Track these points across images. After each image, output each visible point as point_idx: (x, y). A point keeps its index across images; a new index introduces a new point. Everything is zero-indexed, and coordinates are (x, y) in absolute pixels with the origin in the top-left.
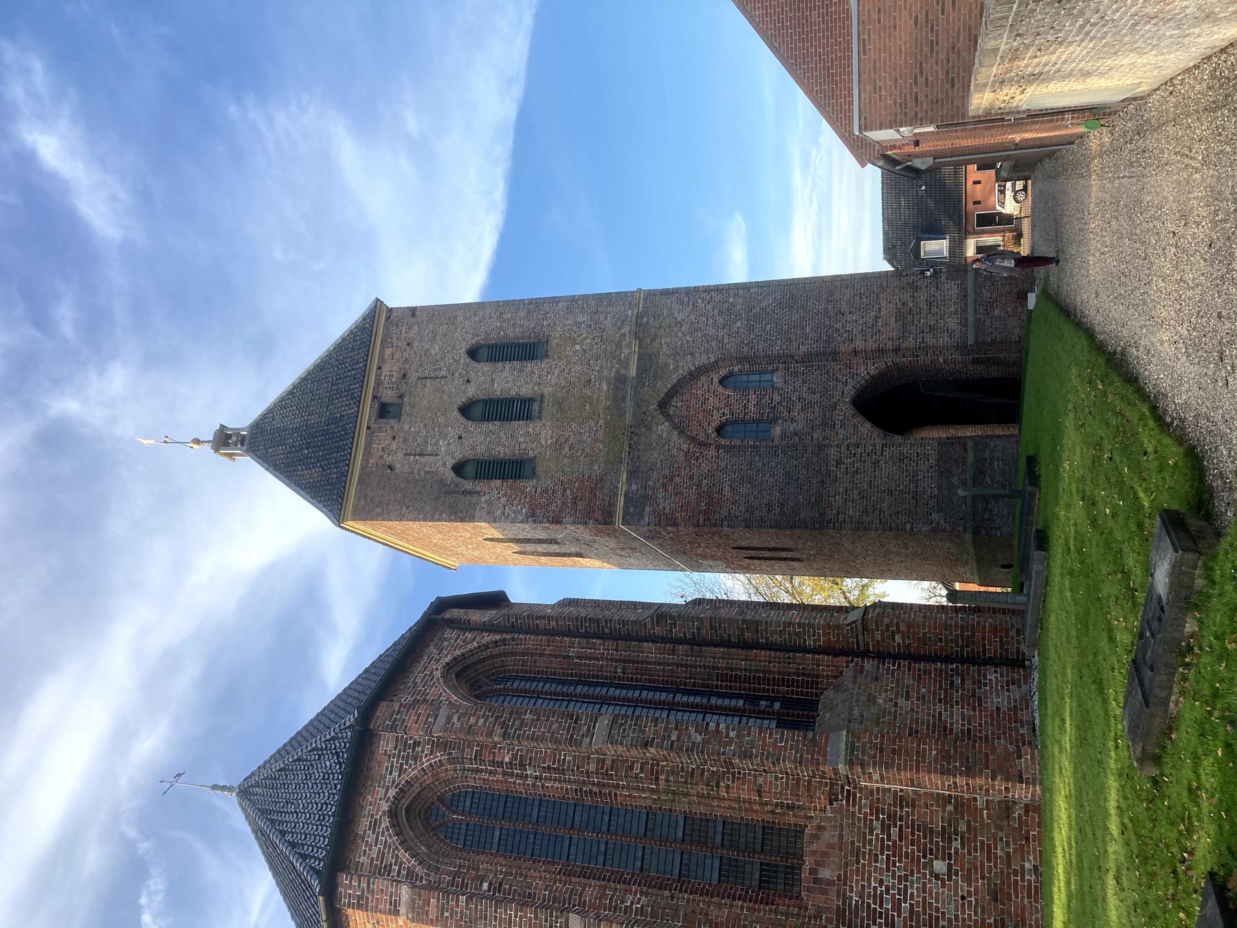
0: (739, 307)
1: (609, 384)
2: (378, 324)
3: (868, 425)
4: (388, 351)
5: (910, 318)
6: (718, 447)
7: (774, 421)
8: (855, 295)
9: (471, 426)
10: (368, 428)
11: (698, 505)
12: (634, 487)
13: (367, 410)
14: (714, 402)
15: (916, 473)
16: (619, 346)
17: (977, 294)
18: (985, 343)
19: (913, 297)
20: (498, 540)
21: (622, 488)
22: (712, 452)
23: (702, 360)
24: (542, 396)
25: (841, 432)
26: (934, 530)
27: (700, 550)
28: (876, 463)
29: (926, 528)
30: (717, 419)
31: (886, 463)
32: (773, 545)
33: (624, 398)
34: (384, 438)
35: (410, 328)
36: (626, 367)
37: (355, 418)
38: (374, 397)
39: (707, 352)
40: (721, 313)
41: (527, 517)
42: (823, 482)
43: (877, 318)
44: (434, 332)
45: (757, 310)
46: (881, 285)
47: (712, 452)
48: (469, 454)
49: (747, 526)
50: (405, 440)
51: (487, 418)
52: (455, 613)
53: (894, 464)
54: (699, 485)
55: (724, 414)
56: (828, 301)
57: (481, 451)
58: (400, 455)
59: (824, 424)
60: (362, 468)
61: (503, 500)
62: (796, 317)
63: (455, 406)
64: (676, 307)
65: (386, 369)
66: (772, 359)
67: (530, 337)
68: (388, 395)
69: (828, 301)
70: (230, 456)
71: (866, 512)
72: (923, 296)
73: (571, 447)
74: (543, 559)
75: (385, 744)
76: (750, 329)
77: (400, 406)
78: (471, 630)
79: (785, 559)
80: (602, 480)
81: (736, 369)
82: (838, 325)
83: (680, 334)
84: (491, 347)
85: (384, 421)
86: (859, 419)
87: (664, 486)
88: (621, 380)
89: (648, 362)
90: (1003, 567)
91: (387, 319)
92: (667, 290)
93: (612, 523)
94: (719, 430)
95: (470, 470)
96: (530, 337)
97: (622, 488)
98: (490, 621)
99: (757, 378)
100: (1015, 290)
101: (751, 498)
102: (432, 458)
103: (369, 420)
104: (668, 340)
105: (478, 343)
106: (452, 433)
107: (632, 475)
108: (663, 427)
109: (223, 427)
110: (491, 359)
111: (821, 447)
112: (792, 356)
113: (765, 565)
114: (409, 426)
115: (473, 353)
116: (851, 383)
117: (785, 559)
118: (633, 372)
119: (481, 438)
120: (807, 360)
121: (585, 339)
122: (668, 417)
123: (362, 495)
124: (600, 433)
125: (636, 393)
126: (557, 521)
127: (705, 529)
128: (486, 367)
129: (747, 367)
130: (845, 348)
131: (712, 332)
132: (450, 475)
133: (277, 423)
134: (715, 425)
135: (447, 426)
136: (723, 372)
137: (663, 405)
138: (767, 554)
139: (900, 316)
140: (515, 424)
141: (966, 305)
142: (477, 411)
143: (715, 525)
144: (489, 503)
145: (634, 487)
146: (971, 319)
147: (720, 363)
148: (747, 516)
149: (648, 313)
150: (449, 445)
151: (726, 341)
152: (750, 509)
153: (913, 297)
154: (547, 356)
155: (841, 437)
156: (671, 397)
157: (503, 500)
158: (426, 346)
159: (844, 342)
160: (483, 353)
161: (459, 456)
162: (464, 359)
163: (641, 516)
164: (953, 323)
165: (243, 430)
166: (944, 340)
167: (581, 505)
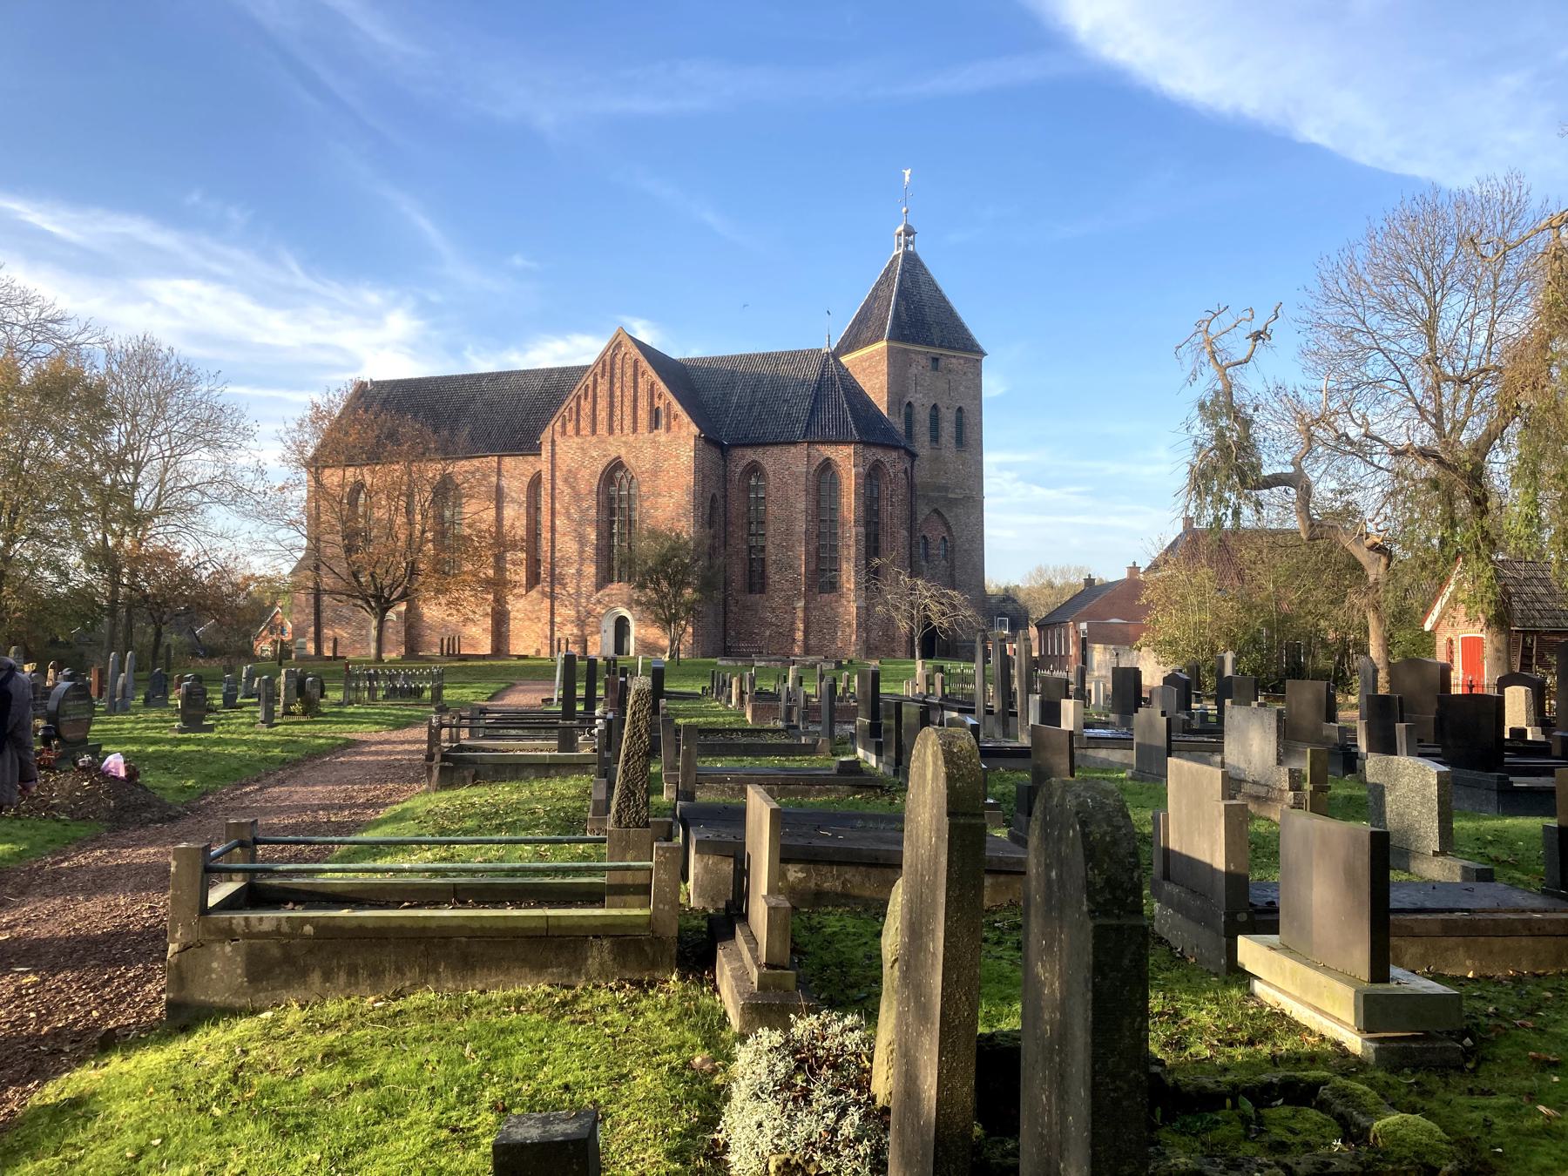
2: (970, 350)
30: (929, 535)
37: (931, 344)
66: (953, 561)
68: (942, 363)
75: (894, 454)
88: (945, 489)
89: (953, 503)
115: (960, 409)
132: (907, 400)
137: (936, 511)
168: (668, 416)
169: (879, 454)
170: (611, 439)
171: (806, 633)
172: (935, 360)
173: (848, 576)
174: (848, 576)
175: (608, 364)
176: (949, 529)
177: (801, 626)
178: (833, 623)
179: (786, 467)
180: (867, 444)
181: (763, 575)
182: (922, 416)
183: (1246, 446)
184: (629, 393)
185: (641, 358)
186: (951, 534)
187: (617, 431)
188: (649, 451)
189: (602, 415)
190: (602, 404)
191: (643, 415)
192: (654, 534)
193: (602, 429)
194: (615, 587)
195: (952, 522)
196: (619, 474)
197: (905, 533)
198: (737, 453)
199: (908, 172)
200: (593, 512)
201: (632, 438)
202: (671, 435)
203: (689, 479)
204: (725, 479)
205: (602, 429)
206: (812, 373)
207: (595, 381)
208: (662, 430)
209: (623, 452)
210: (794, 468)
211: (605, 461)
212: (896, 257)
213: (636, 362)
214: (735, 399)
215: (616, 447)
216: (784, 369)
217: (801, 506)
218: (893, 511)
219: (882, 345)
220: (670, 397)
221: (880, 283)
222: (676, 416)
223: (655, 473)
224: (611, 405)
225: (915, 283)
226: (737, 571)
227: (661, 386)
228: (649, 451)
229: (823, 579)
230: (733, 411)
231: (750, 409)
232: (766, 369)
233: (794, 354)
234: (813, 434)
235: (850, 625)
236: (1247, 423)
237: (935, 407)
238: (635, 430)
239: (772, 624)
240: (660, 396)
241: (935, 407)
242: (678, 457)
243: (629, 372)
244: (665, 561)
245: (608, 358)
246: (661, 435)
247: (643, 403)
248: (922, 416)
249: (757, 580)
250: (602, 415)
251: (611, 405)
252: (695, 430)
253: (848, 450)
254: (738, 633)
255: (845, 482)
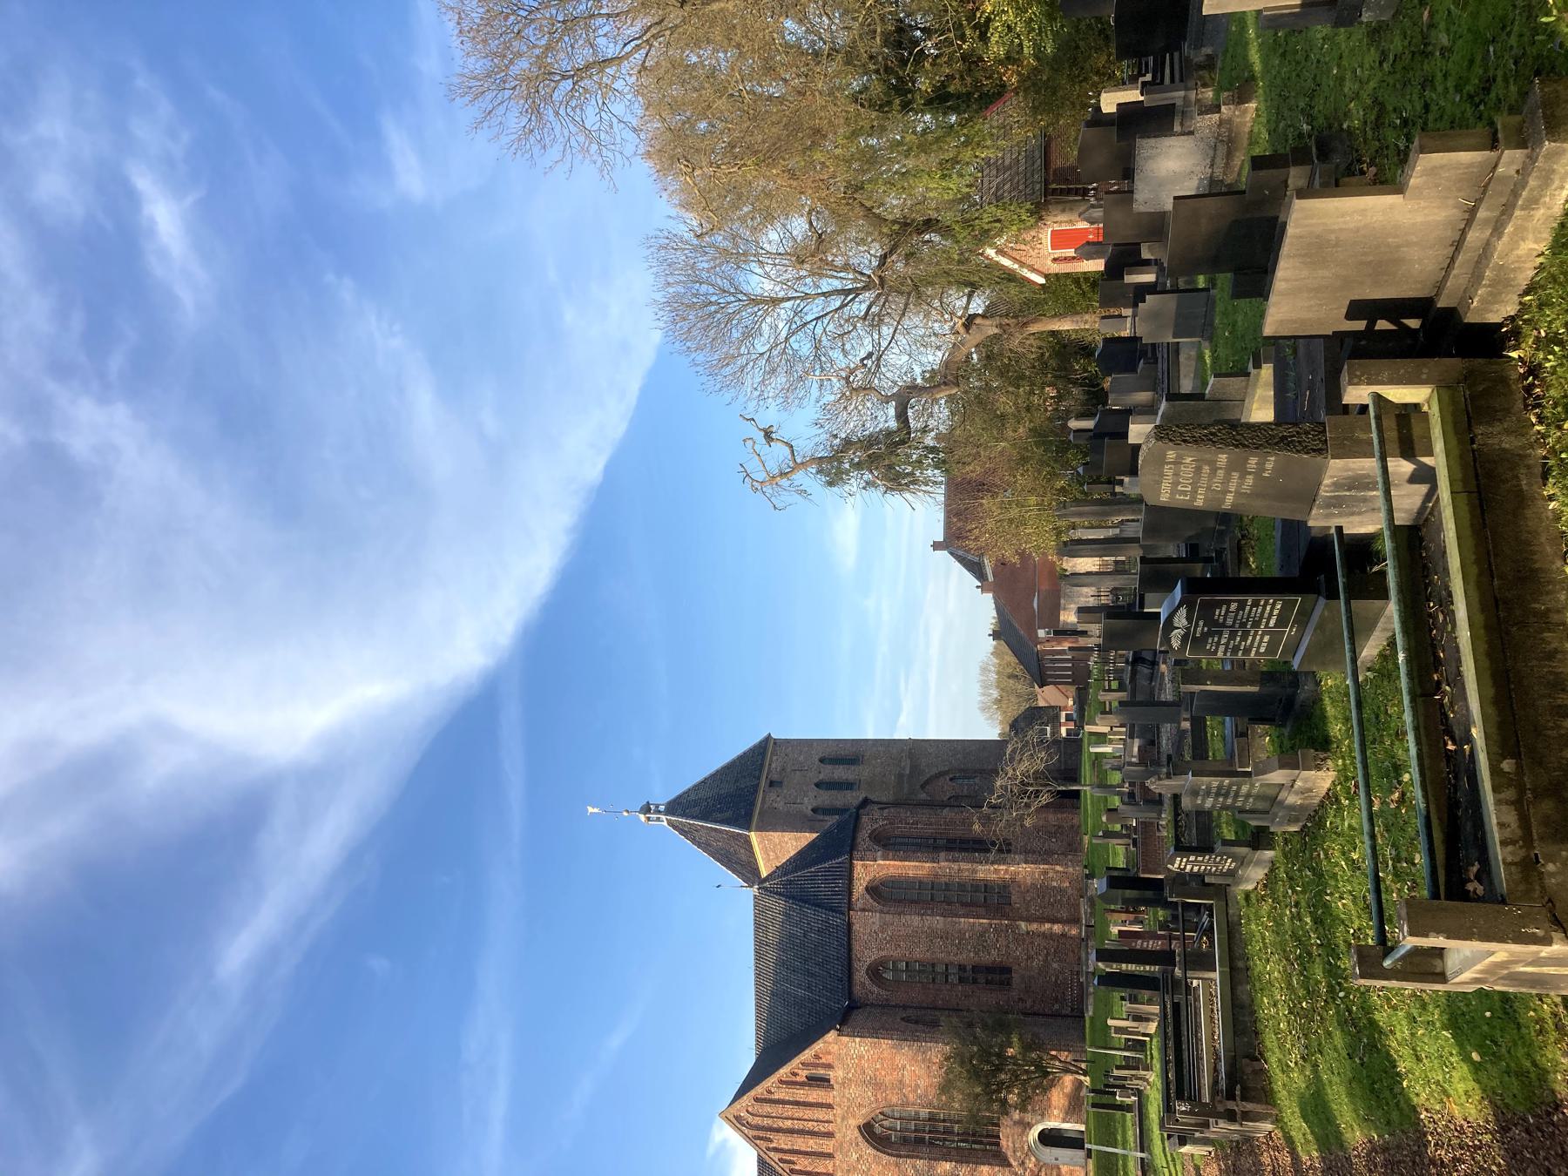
2: (766, 747)
37: (756, 788)
68: (775, 777)
75: (864, 819)
88: (900, 776)
89: (915, 768)
115: (822, 760)
132: (810, 813)
133: (693, 797)
137: (923, 787)
168: (816, 1066)
169: (864, 835)
170: (838, 1135)
171: (1054, 921)
173: (989, 871)
174: (989, 871)
175: (757, 1133)
176: (942, 774)
177: (1047, 926)
178: (1041, 890)
179: (874, 935)
180: (853, 847)
181: (990, 969)
182: (826, 798)
183: (870, 442)
184: (790, 1111)
185: (752, 1093)
187: (830, 1127)
188: (853, 1091)
189: (812, 1144)
190: (801, 1143)
191: (814, 1095)
192: (945, 1087)
193: (827, 1146)
194: (1006, 1143)
195: (934, 771)
196: (878, 1129)
197: (946, 811)
198: (857, 990)
199: (590, 810)
200: (919, 1163)
201: (838, 1111)
202: (836, 1063)
203: (885, 1044)
204: (885, 1006)
205: (827, 1146)
206: (777, 905)
207: (776, 1150)
208: (831, 1074)
209: (853, 1122)
210: (876, 927)
211: (863, 1145)
212: (669, 822)
213: (757, 1100)
214: (801, 992)
215: (848, 1130)
216: (773, 936)
217: (915, 920)
218: (923, 822)
219: (753, 836)
220: (796, 1062)
221: (694, 841)
222: (817, 1056)
223: (877, 1085)
224: (801, 1132)
225: (696, 803)
226: (991, 998)
227: (783, 1072)
228: (853, 1091)
229: (994, 900)
230: (813, 994)
231: (812, 975)
232: (772, 956)
233: (758, 925)
234: (841, 904)
235: (1045, 873)
236: (847, 443)
237: (817, 785)
238: (829, 1106)
239: (1045, 961)
240: (795, 1074)
241: (817, 785)
242: (861, 1057)
243: (768, 1108)
244: (975, 1074)
245: (751, 1133)
246: (836, 1075)
247: (801, 1094)
248: (826, 798)
249: (998, 975)
250: (812, 1144)
251: (801, 1132)
252: (831, 1036)
253: (858, 864)
254: (1056, 1000)
255: (892, 871)
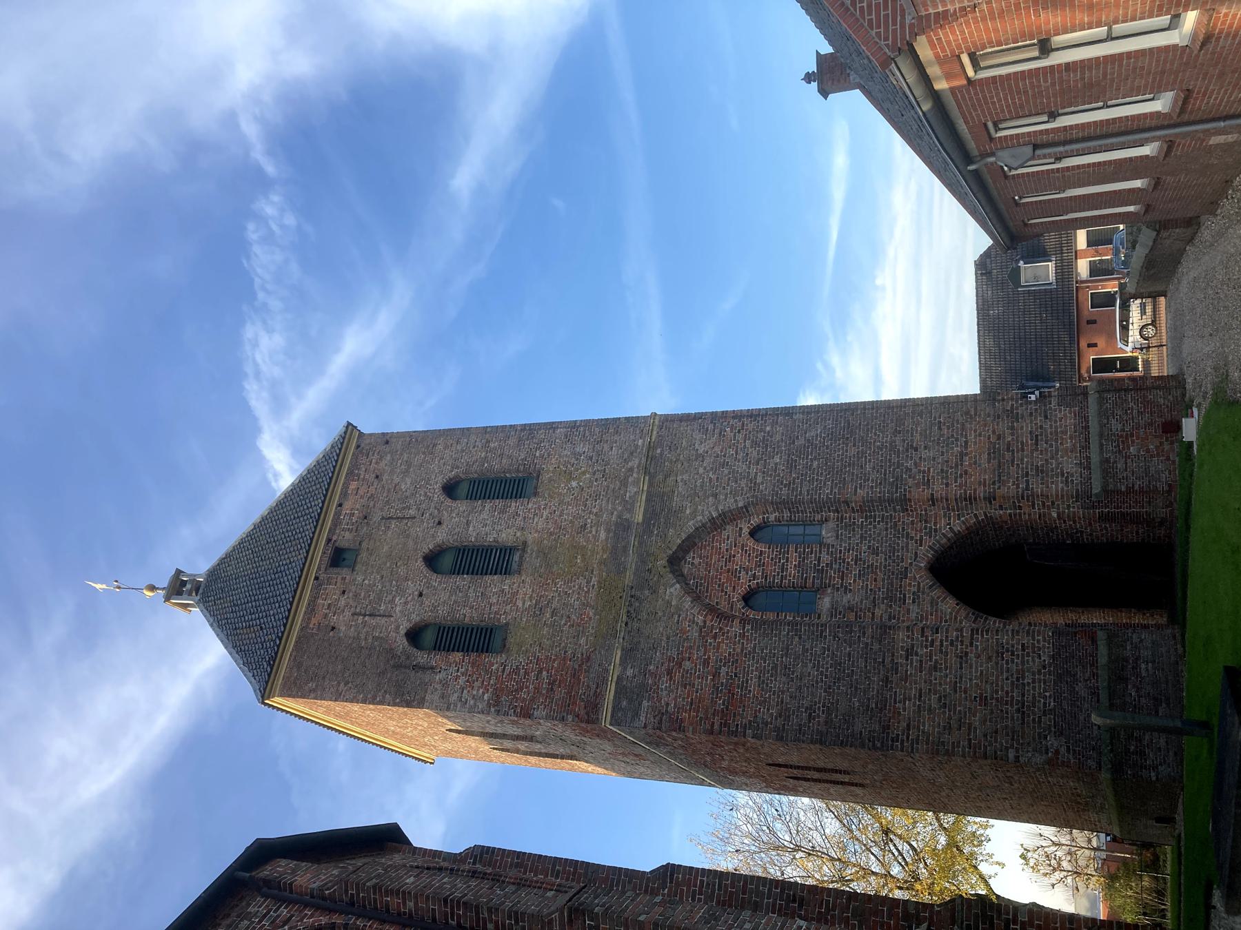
0: (778, 437)
1: (608, 531)
3: (951, 601)
4: (353, 485)
5: (1008, 455)
6: (744, 621)
7: (821, 589)
8: (932, 425)
9: (435, 580)
10: (316, 578)
11: (714, 703)
12: (630, 672)
13: (320, 554)
14: (742, 560)
15: (1021, 674)
16: (624, 483)
17: (1102, 426)
18: (1119, 492)
19: (1012, 428)
20: (458, 732)
21: (614, 672)
22: (736, 628)
23: (729, 504)
24: (525, 543)
25: (914, 609)
26: (1049, 762)
27: (725, 764)
28: (963, 656)
29: (1039, 759)
30: (745, 583)
31: (978, 656)
32: (821, 764)
33: (625, 549)
34: (333, 590)
35: (381, 459)
36: (631, 510)
38: (329, 540)
39: (734, 493)
40: (755, 444)
41: (489, 705)
42: (886, 680)
43: (962, 455)
44: (409, 464)
45: (801, 441)
46: (967, 413)
47: (736, 628)
48: (428, 616)
49: (780, 738)
50: (356, 595)
51: (457, 570)
52: (280, 868)
53: (990, 658)
54: (716, 674)
55: (754, 576)
56: (896, 432)
57: (442, 611)
58: (347, 613)
59: (890, 598)
60: (302, 629)
61: (462, 681)
62: (853, 451)
63: (420, 554)
64: (698, 436)
65: (347, 505)
66: (820, 506)
67: (518, 471)
68: (345, 538)
69: (896, 432)
70: (185, 606)
71: (948, 728)
72: (1026, 427)
73: (553, 613)
74: (533, 759)
76: (791, 465)
77: (357, 552)
78: (289, 902)
79: (842, 783)
80: (588, 659)
81: (772, 517)
82: (910, 464)
83: (701, 470)
84: (473, 482)
85: (336, 570)
86: (938, 592)
87: (669, 672)
88: (623, 526)
90: (1158, 820)
91: (358, 447)
92: (689, 415)
93: (596, 721)
94: (747, 599)
95: (429, 637)
96: (518, 471)
97: (614, 672)
98: (321, 889)
99: (800, 530)
100: (1159, 421)
101: (786, 698)
102: (385, 619)
103: (319, 568)
104: (685, 477)
105: (457, 476)
106: (412, 588)
107: (629, 654)
108: (674, 591)
109: (179, 572)
110: (471, 496)
111: (885, 629)
112: (847, 503)
113: (816, 787)
114: (362, 577)
115: (450, 489)
116: (929, 541)
117: (842, 783)
118: (639, 517)
119: (444, 596)
120: (866, 508)
121: (584, 473)
122: (680, 577)
123: (297, 664)
124: (592, 595)
125: (640, 543)
126: (526, 714)
127: (723, 738)
128: (462, 506)
129: (786, 514)
130: (919, 494)
131: (741, 467)
132: (402, 643)
134: (741, 590)
135: (407, 579)
136: (755, 521)
137: (675, 562)
138: (816, 775)
139: (993, 452)
140: (488, 578)
141: (1087, 440)
142: (448, 561)
143: (735, 733)
144: (445, 684)
145: (630, 672)
146: (1095, 458)
147: (751, 509)
148: (779, 722)
149: (662, 442)
150: (406, 603)
151: (759, 480)
152: (784, 714)
153: (1012, 428)
154: (536, 494)
155: (913, 616)
156: (687, 552)
157: (462, 681)
158: (397, 480)
159: (918, 485)
160: (463, 489)
161: (415, 618)
162: (438, 496)
163: (636, 715)
164: (1070, 464)
165: (200, 576)
166: (1057, 486)
167: (560, 693)
172: (338, 558)
176: (717, 524)
186: (743, 513)
195: (709, 510)
237: (432, 560)
241: (432, 560)
